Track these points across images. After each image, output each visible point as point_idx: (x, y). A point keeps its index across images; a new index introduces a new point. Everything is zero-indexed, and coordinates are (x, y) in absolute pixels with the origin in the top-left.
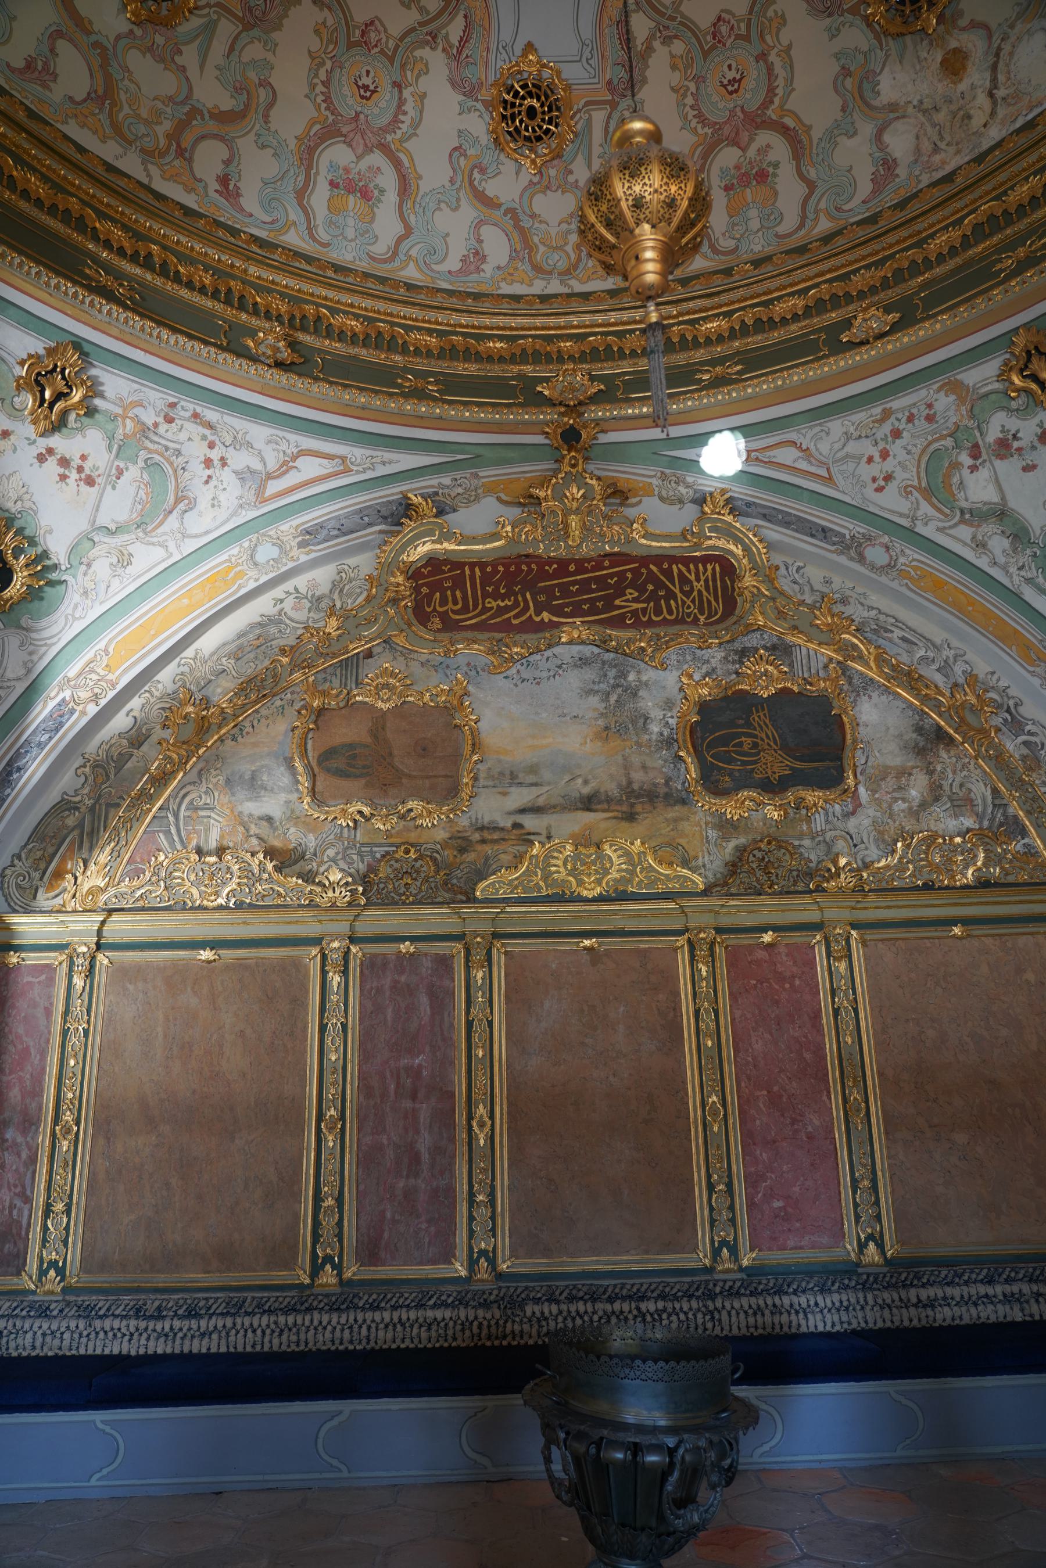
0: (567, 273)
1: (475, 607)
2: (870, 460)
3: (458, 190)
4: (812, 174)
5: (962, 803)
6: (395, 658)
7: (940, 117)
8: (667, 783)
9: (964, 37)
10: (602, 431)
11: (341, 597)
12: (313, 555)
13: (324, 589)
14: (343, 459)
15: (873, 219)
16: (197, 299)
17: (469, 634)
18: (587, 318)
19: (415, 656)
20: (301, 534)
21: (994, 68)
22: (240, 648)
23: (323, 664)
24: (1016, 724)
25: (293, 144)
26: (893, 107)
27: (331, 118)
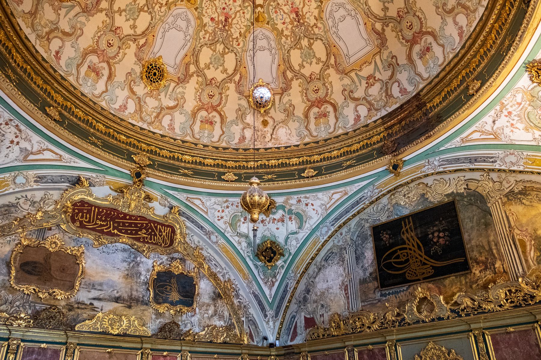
0: (150, 124)
1: (93, 222)
2: (219, 211)
3: (126, 85)
4: (224, 130)
5: (221, 317)
6: (59, 233)
7: (259, 133)
8: (143, 297)
9: (269, 118)
10: (148, 177)
11: (43, 204)
12: (39, 187)
13: (37, 199)
14: (61, 156)
15: (237, 150)
16: (36, 88)
17: (88, 231)
18: (152, 141)
19: (67, 234)
20: (36, 177)
21: (274, 130)
23: (31, 228)
24: (237, 296)
25: (82, 50)
26: (248, 124)
27: (96, 47)
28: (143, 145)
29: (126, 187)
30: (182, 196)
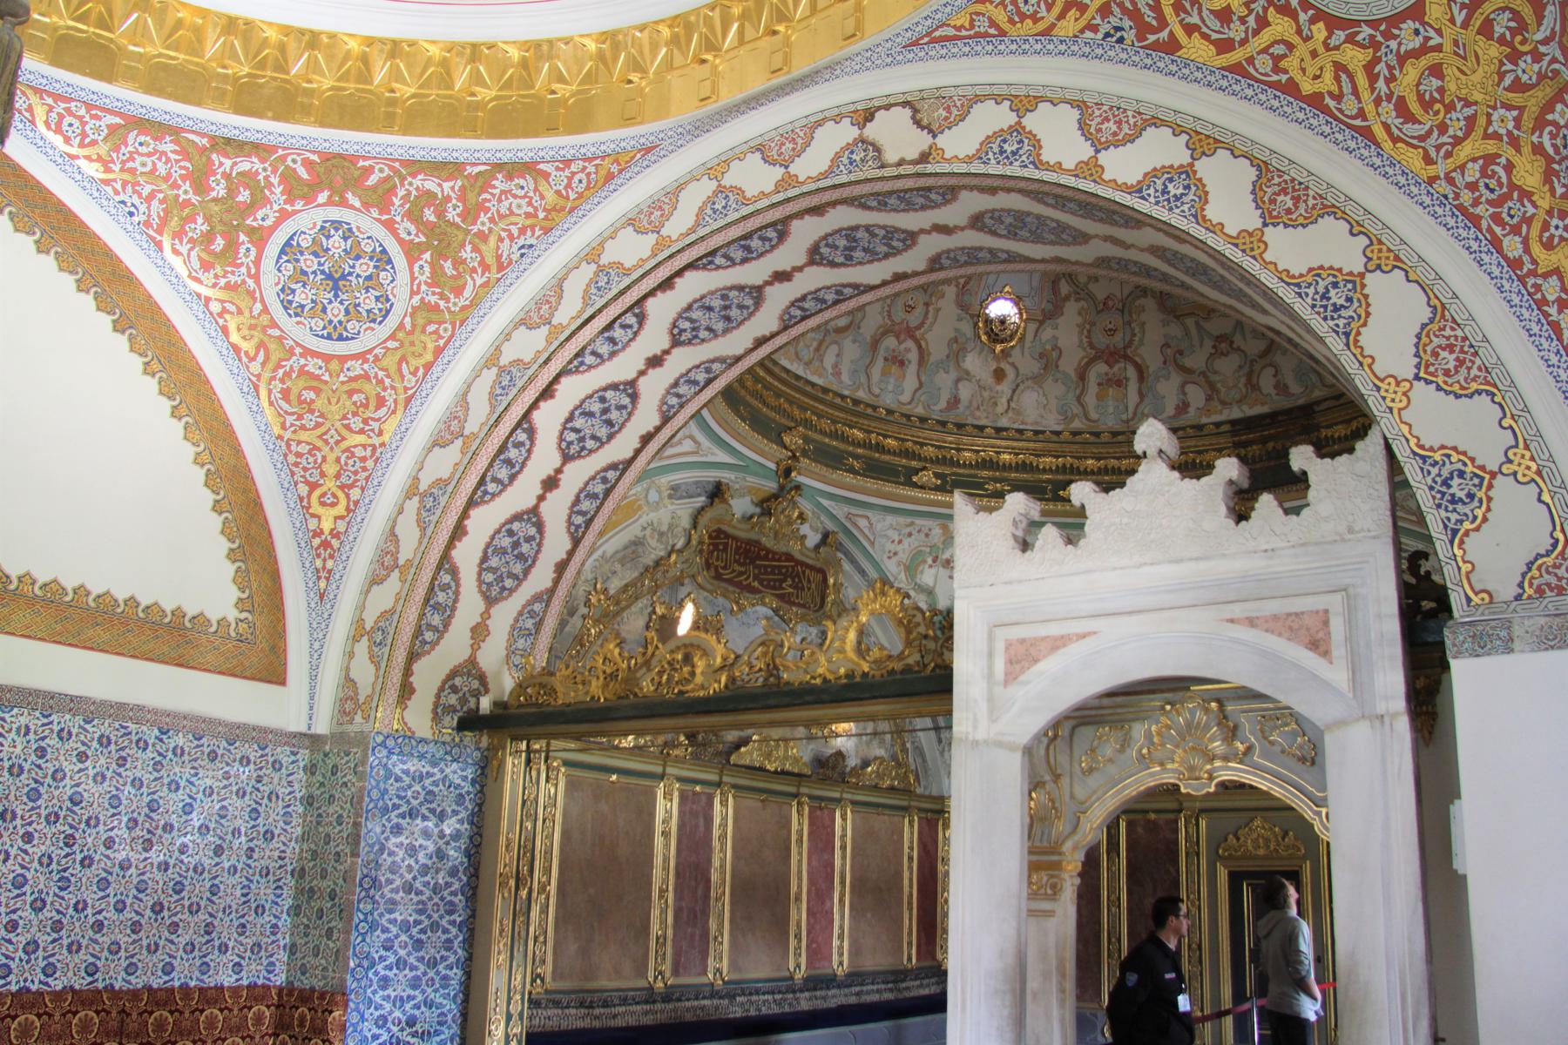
7: (986, 394)
13: (664, 528)
15: (943, 424)
22: (624, 557)
26: (967, 373)
28: (796, 412)
29: (775, 497)
30: (840, 511)
